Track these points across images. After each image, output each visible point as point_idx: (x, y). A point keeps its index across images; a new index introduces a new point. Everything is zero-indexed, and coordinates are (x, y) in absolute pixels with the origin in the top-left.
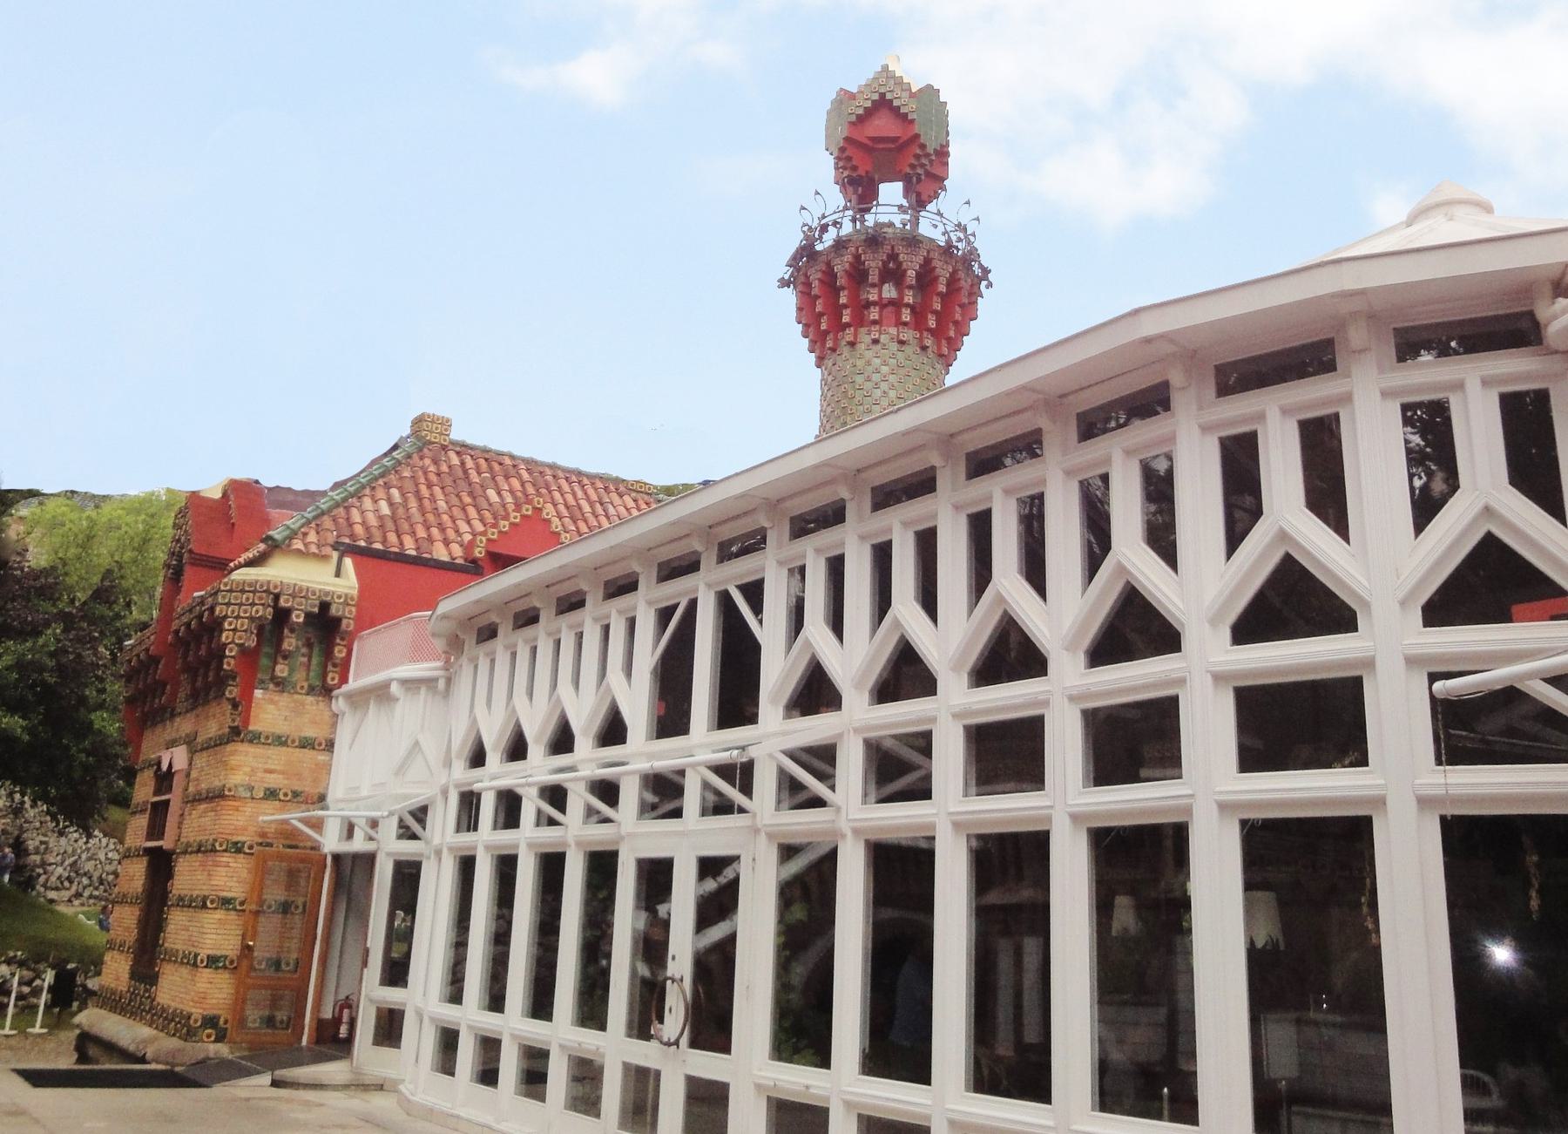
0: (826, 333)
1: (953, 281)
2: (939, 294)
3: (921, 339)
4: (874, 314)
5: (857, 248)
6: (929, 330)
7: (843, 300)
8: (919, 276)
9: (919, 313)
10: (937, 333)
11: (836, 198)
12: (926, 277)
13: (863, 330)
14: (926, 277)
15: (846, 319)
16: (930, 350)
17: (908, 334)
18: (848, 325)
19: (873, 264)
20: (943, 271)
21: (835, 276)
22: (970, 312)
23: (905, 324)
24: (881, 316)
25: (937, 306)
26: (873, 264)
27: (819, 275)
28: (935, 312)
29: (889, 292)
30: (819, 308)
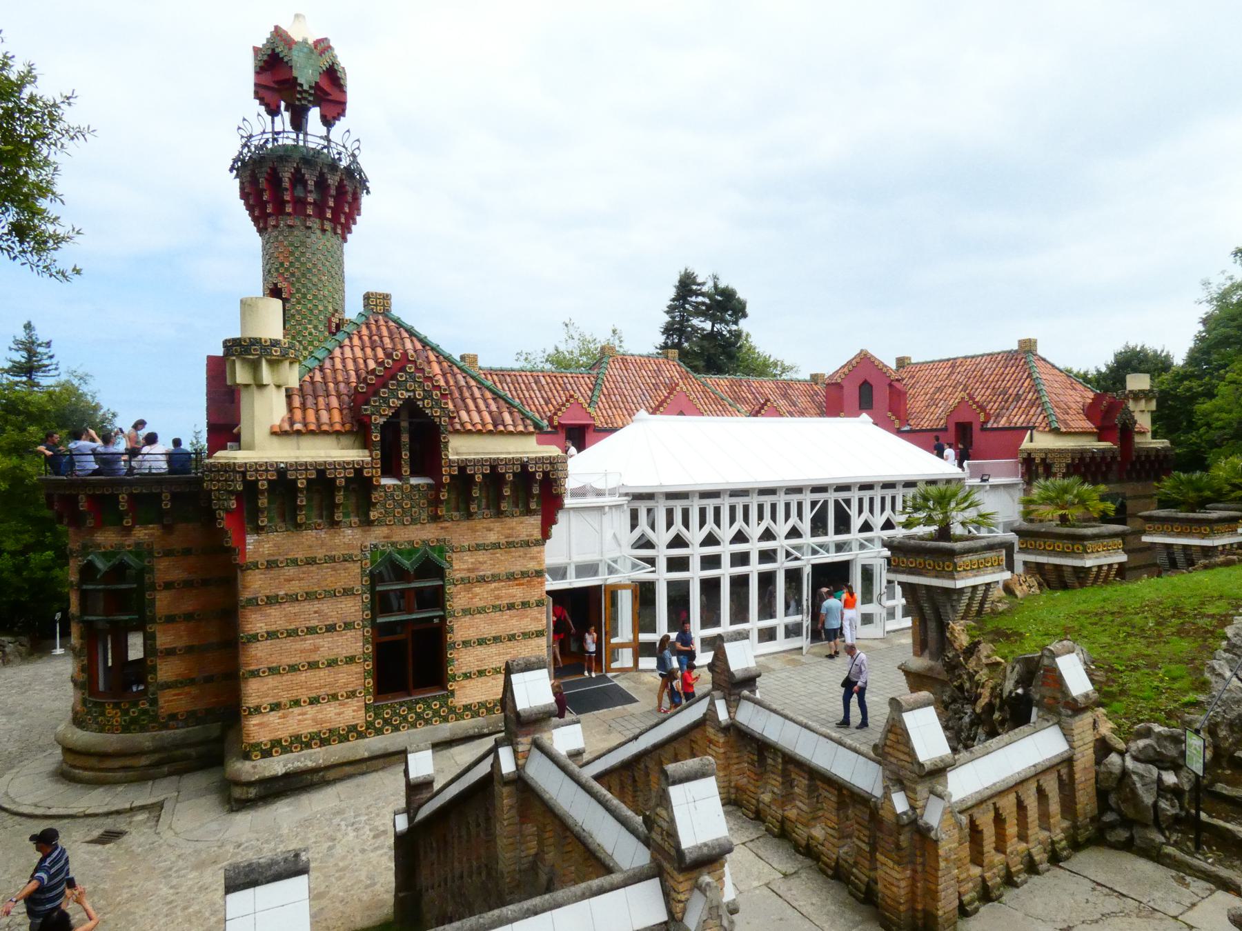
1: (341, 187)
3: (323, 225)
7: (265, 198)
9: (320, 208)
10: (335, 220)
12: (322, 184)
14: (322, 184)
18: (269, 215)
19: (286, 176)
20: (333, 181)
22: (355, 208)
23: (310, 215)
25: (331, 204)
26: (286, 176)
28: (330, 207)
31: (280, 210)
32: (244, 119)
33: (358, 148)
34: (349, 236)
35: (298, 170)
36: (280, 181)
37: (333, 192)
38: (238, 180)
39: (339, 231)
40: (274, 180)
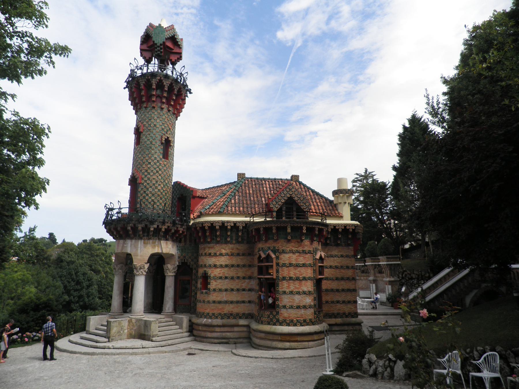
0: (137, 104)
2: (175, 94)
3: (168, 108)
4: (154, 99)
5: (148, 77)
6: (171, 105)
8: (169, 88)
10: (174, 107)
11: (141, 61)
13: (149, 103)
14: (171, 87)
15: (144, 99)
16: (171, 112)
17: (165, 106)
18: (144, 102)
19: (154, 82)
21: (140, 86)
24: (156, 99)
25: (174, 98)
26: (154, 82)
27: (135, 85)
29: (159, 92)
30: (135, 96)
31: (149, 98)
32: (135, 59)
33: (187, 78)
34: (179, 118)
35: (160, 81)
36: (151, 85)
37: (176, 92)
38: (127, 89)
39: (176, 112)
40: (148, 85)
